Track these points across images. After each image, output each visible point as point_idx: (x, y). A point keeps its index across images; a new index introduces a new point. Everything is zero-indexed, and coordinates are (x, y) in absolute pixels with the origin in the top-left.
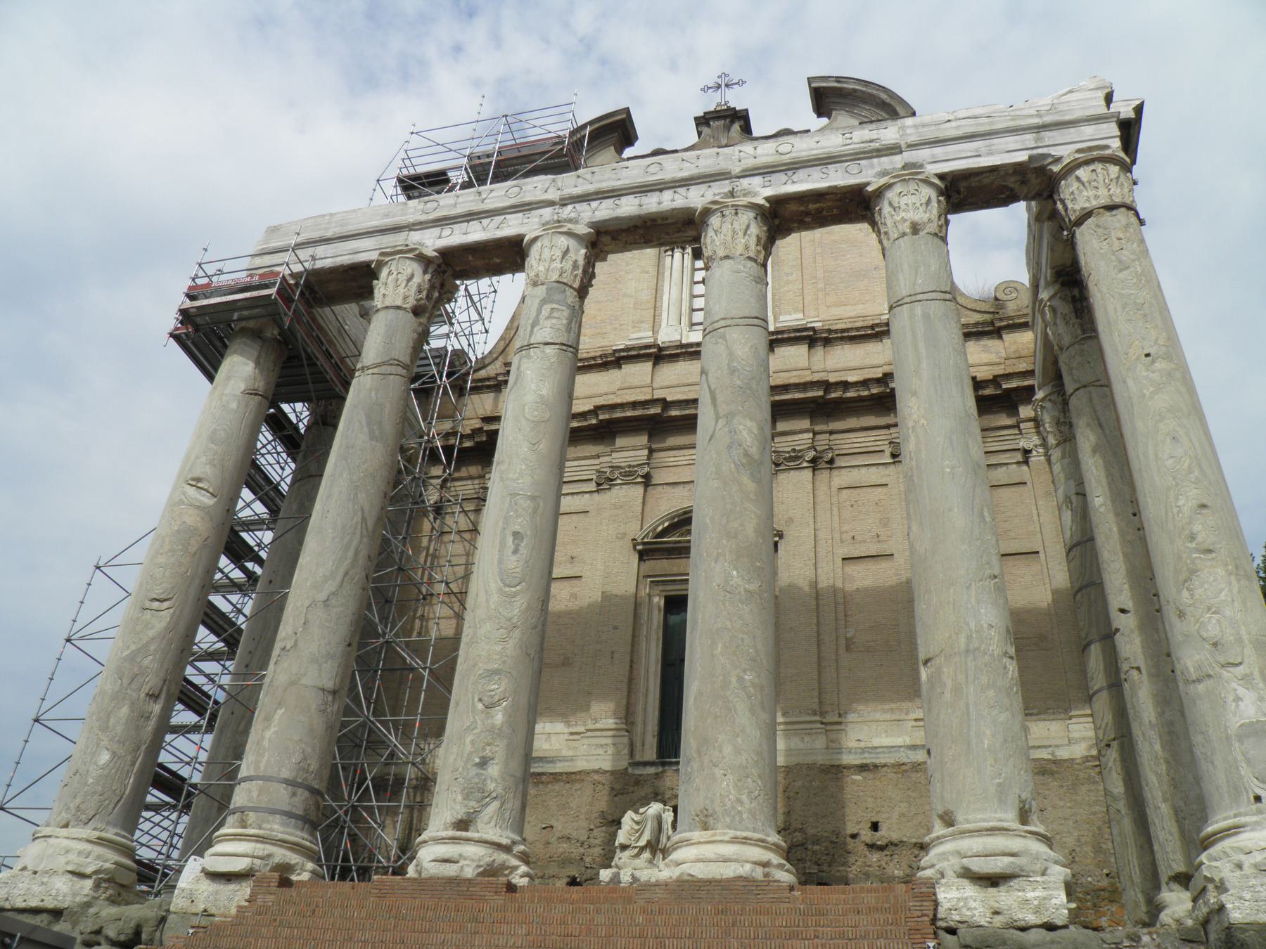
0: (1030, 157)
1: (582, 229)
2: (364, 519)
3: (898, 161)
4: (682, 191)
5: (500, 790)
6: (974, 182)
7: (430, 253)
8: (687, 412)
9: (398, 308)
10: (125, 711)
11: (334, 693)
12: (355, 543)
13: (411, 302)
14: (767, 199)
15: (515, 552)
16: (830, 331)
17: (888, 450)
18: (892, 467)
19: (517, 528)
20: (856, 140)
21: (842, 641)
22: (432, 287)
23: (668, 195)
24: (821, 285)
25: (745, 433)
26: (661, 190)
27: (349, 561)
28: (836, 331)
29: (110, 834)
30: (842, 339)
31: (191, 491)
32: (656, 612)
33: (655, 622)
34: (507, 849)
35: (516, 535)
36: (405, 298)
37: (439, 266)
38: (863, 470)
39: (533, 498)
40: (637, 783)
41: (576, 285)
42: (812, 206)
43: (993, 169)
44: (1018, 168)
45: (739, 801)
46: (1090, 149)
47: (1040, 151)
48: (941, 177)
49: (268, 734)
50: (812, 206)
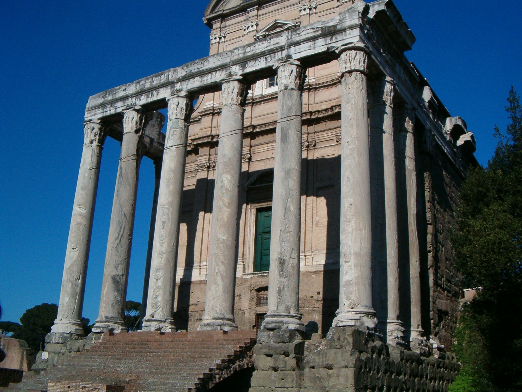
0: (328, 49)
1: (183, 93)
2: (125, 216)
3: (285, 53)
4: (214, 73)
5: (162, 305)
7: (137, 107)
8: (262, 129)
9: (129, 132)
11: (123, 275)
12: (123, 225)
13: (134, 129)
14: (241, 75)
15: (163, 228)
16: (316, 84)
17: (335, 138)
18: (337, 147)
19: (163, 220)
20: (272, 43)
21: (314, 223)
22: (141, 119)
25: (226, 181)
26: (208, 73)
27: (122, 232)
28: (319, 84)
29: (71, 321)
30: (322, 87)
32: (253, 215)
33: (253, 219)
35: (164, 222)
36: (132, 127)
38: (326, 149)
40: (245, 281)
41: (183, 118)
44: (324, 53)
46: (346, 45)
47: (331, 45)
48: (298, 60)
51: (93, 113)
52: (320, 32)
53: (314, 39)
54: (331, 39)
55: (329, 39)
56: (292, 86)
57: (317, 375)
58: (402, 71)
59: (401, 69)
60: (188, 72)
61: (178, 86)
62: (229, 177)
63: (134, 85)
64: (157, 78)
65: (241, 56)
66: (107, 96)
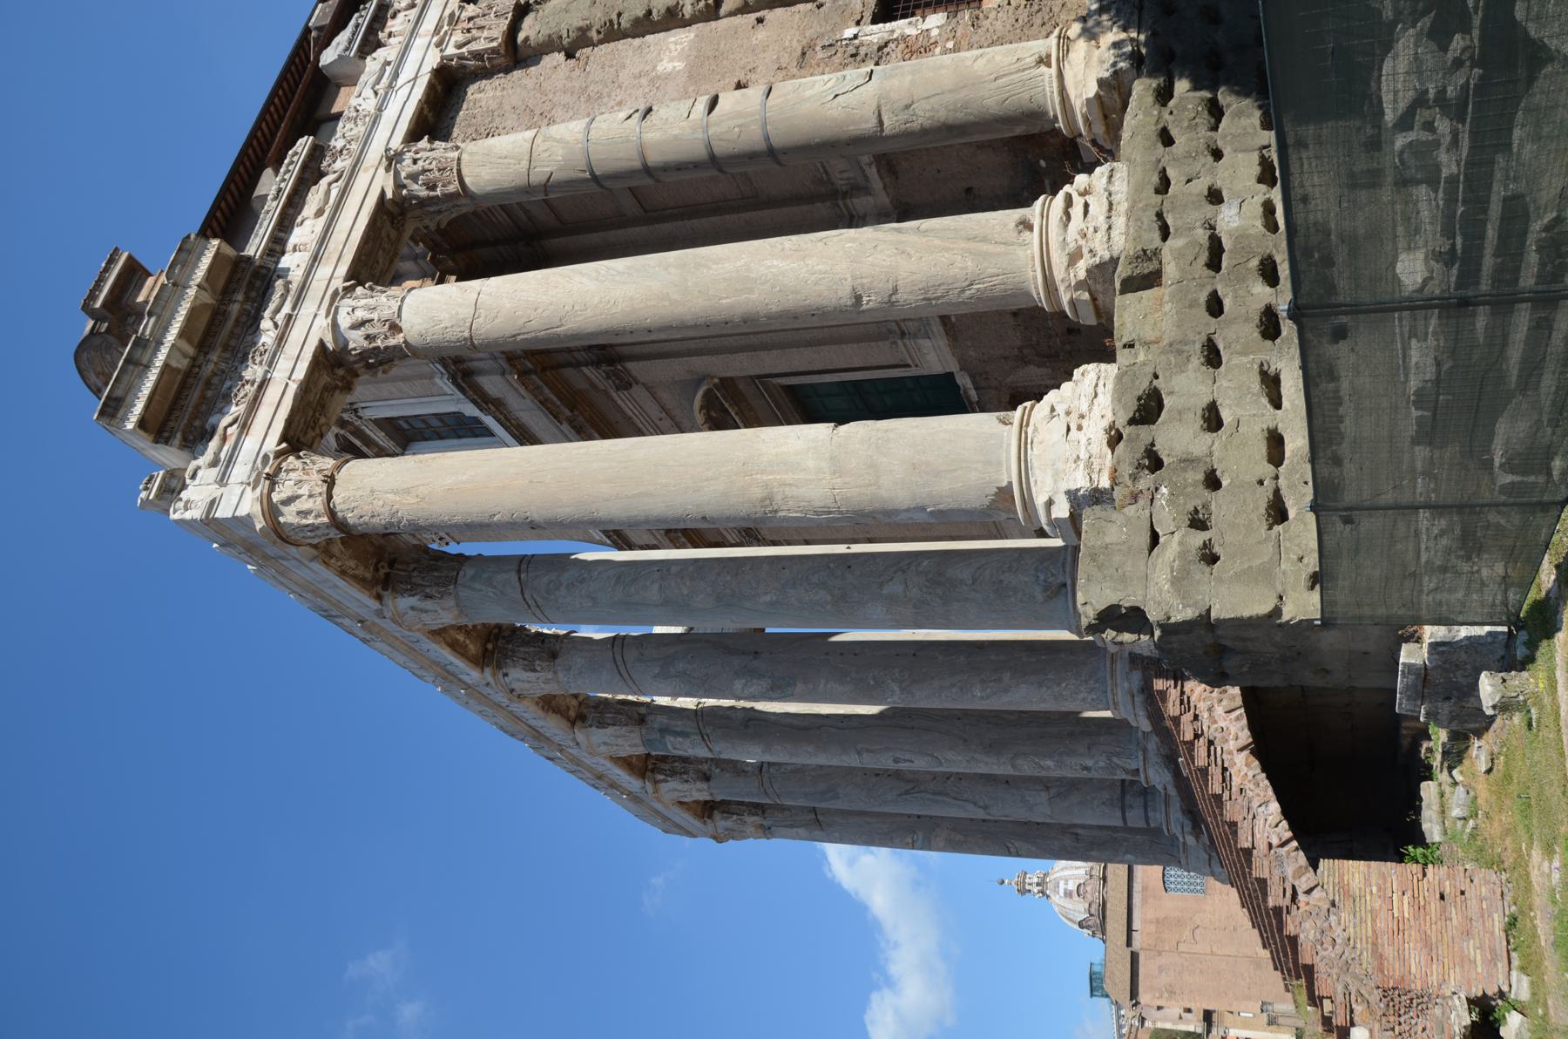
0: (311, 560)
2: (907, 792)
6: (360, 571)
10: (1093, 853)
13: (700, 785)
22: (673, 773)
31: (918, 844)
34: (1145, 750)
35: (896, 761)
37: (653, 771)
39: (859, 753)
41: (636, 729)
42: (461, 638)
43: (343, 573)
45: (1084, 700)
48: (379, 598)
50: (461, 638)
56: (450, 602)
57: (1245, 669)
58: (297, 236)
59: (290, 246)
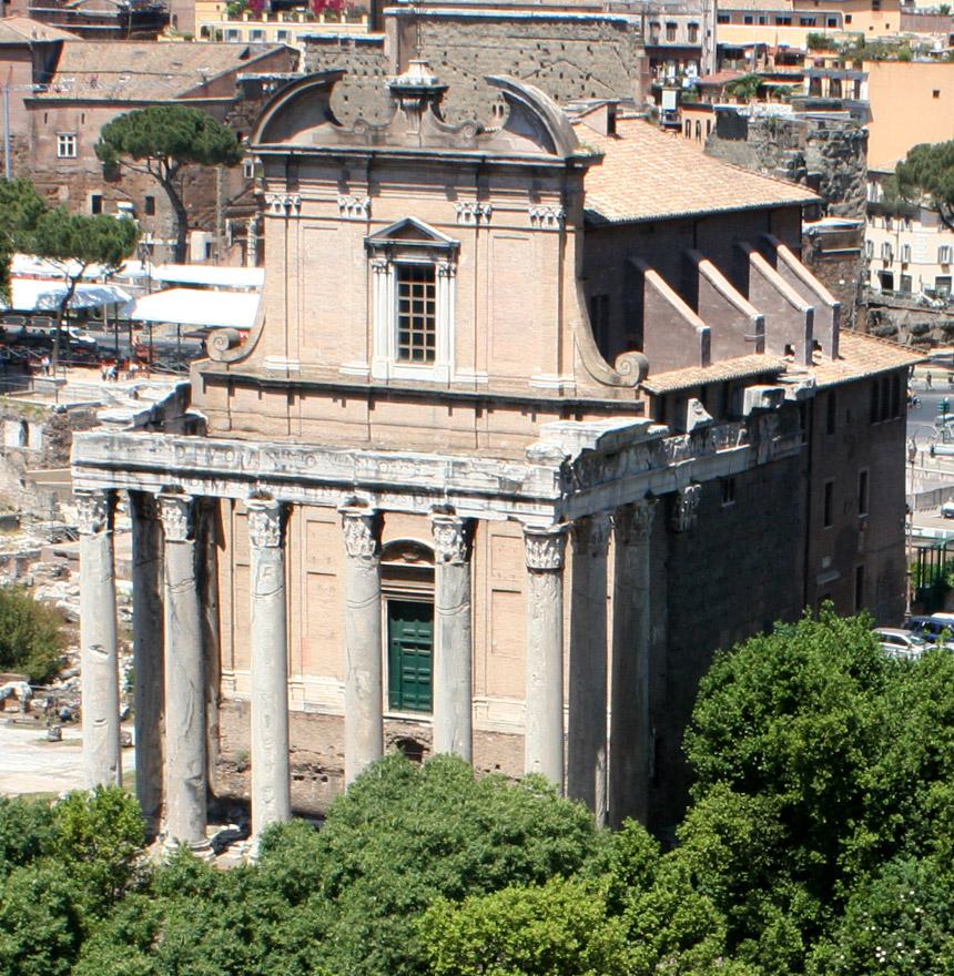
3: (443, 502)
20: (422, 473)
21: (489, 648)
23: (320, 491)
24: (490, 334)
36: (181, 531)
48: (462, 518)
49: (177, 803)
51: (90, 472)
52: (494, 488)
53: (489, 496)
54: (514, 506)
55: (510, 504)
60: (279, 467)
61: (262, 487)
62: (368, 674)
63: (173, 448)
64: (218, 454)
65: (373, 474)
66: (116, 448)
